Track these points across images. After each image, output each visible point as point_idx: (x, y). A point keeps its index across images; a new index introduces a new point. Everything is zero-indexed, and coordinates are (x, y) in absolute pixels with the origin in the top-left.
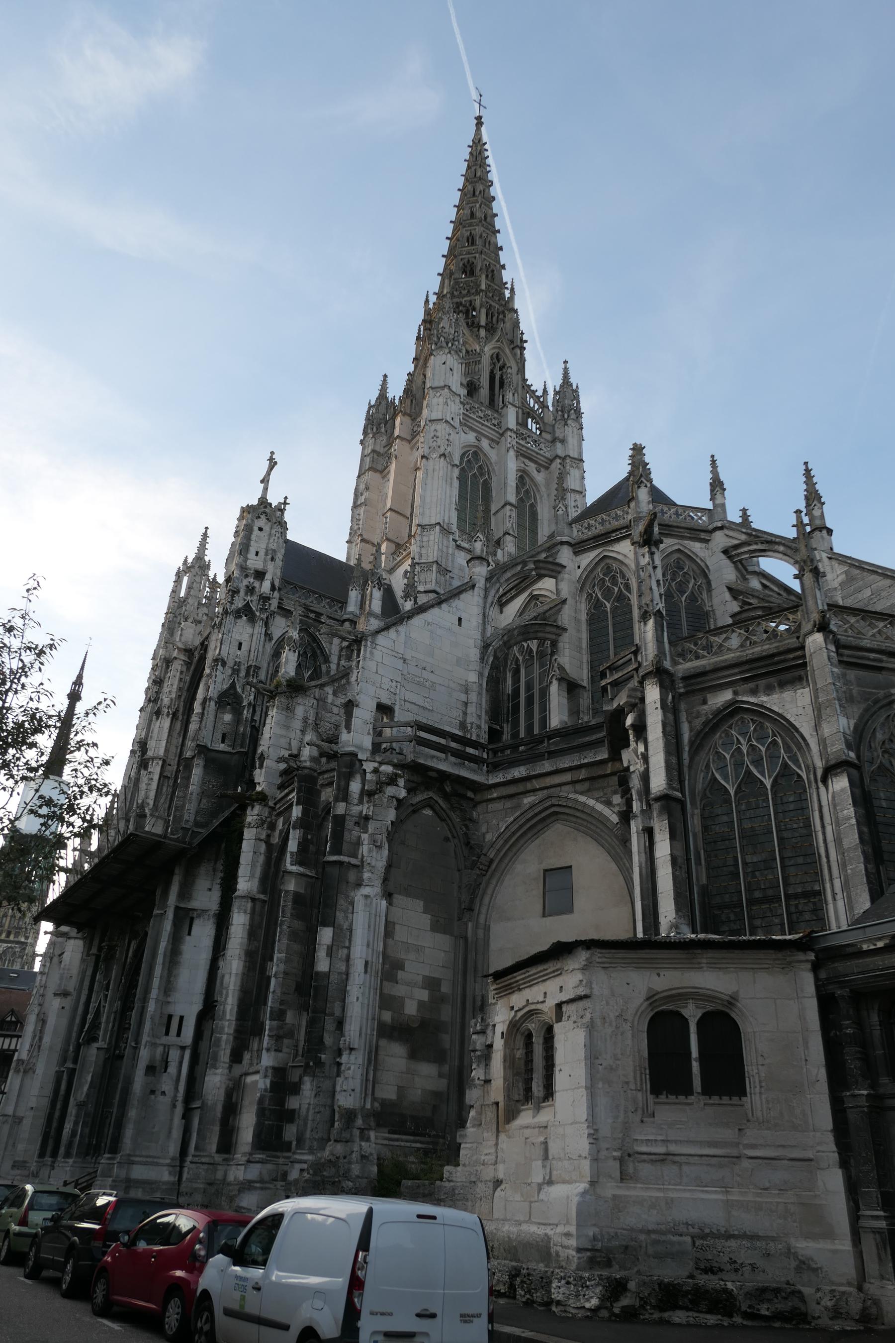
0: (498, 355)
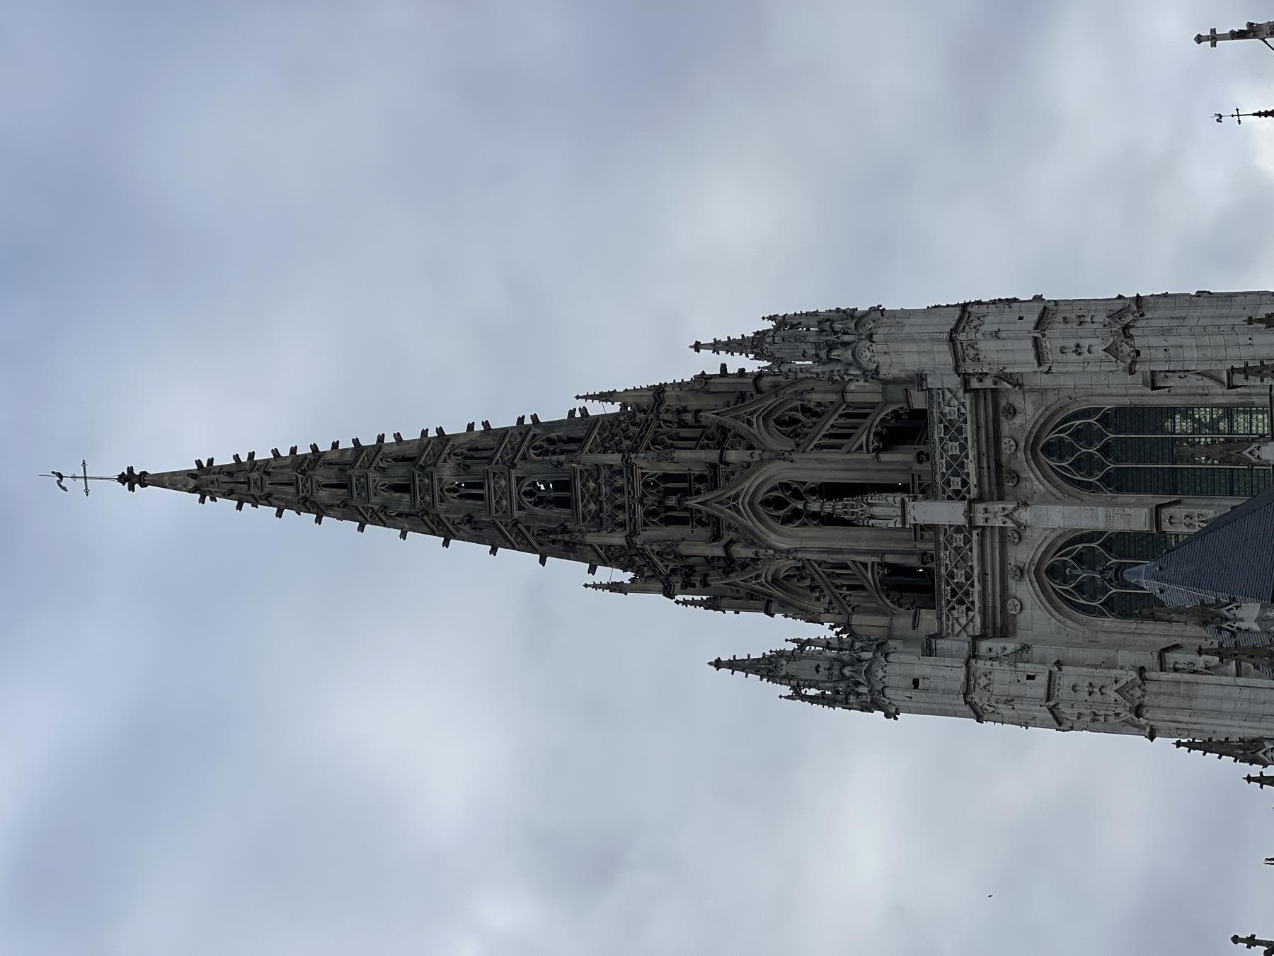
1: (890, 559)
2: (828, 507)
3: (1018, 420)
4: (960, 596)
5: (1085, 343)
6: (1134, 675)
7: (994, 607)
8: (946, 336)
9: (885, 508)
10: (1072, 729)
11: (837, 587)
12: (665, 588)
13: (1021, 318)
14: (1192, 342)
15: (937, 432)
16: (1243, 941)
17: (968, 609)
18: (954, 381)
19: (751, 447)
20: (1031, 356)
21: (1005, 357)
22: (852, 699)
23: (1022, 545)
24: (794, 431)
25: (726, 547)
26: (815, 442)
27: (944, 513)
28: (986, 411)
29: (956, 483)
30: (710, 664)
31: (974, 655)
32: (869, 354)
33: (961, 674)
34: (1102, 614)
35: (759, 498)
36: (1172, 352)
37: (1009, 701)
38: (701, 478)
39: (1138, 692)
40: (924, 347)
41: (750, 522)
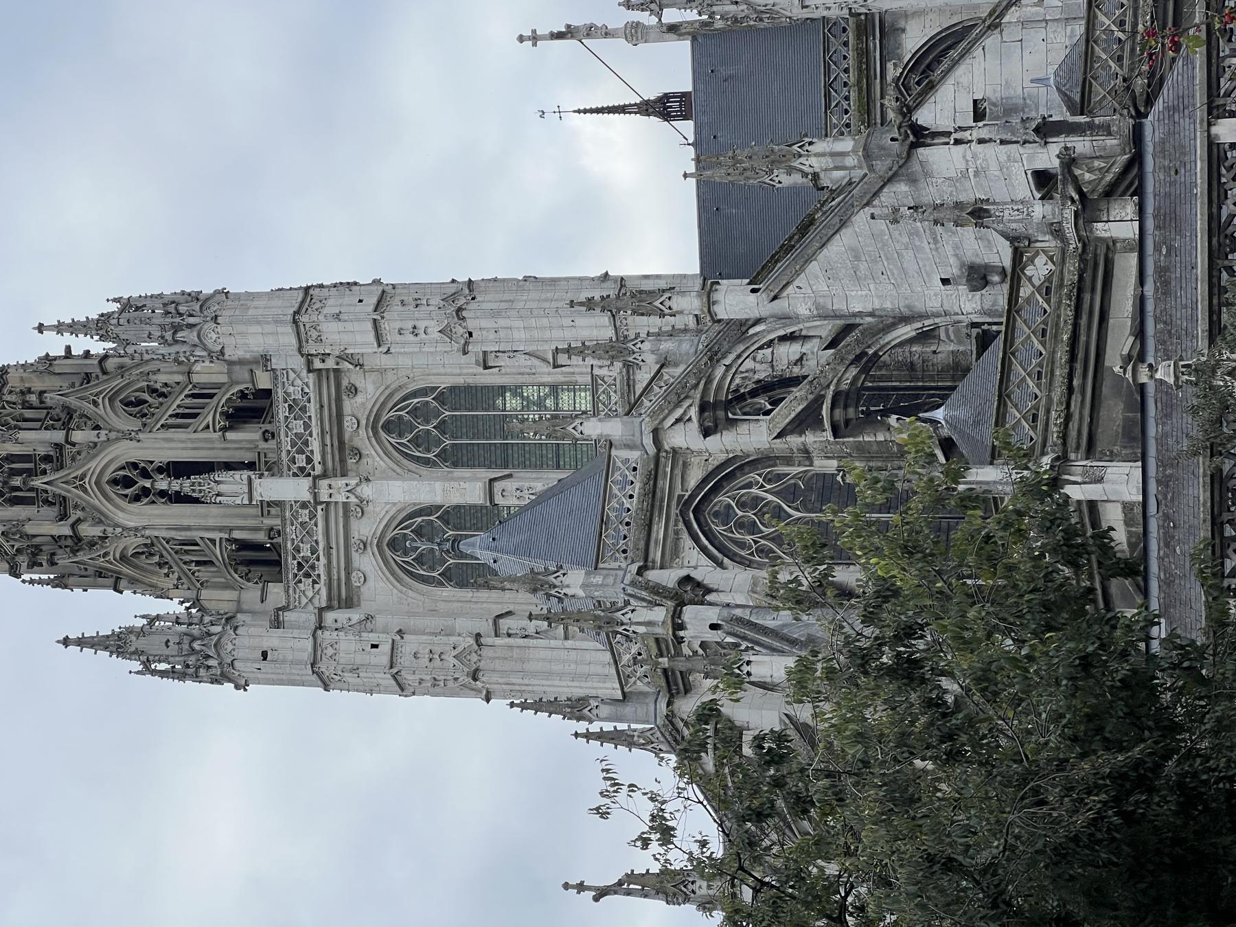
0: (114, 482)
1: (237, 535)
2: (176, 485)
3: (359, 399)
4: (306, 569)
5: (421, 325)
6: (471, 641)
7: (339, 579)
8: (290, 318)
9: (232, 484)
10: (414, 694)
11: (185, 563)
12: (12, 567)
13: (360, 301)
14: (519, 323)
15: (282, 411)
16: (573, 887)
17: (314, 582)
18: (298, 362)
19: (97, 427)
20: (371, 337)
21: (346, 338)
22: (202, 672)
23: (364, 519)
24: (141, 411)
25: (73, 526)
26: (162, 422)
27: (290, 489)
28: (329, 391)
29: (301, 460)
30: (58, 642)
31: (320, 627)
32: (214, 336)
33: (309, 645)
34: (441, 584)
35: (106, 478)
36: (502, 334)
37: (355, 670)
38: (47, 459)
39: (474, 658)
40: (269, 328)
41: (97, 500)
